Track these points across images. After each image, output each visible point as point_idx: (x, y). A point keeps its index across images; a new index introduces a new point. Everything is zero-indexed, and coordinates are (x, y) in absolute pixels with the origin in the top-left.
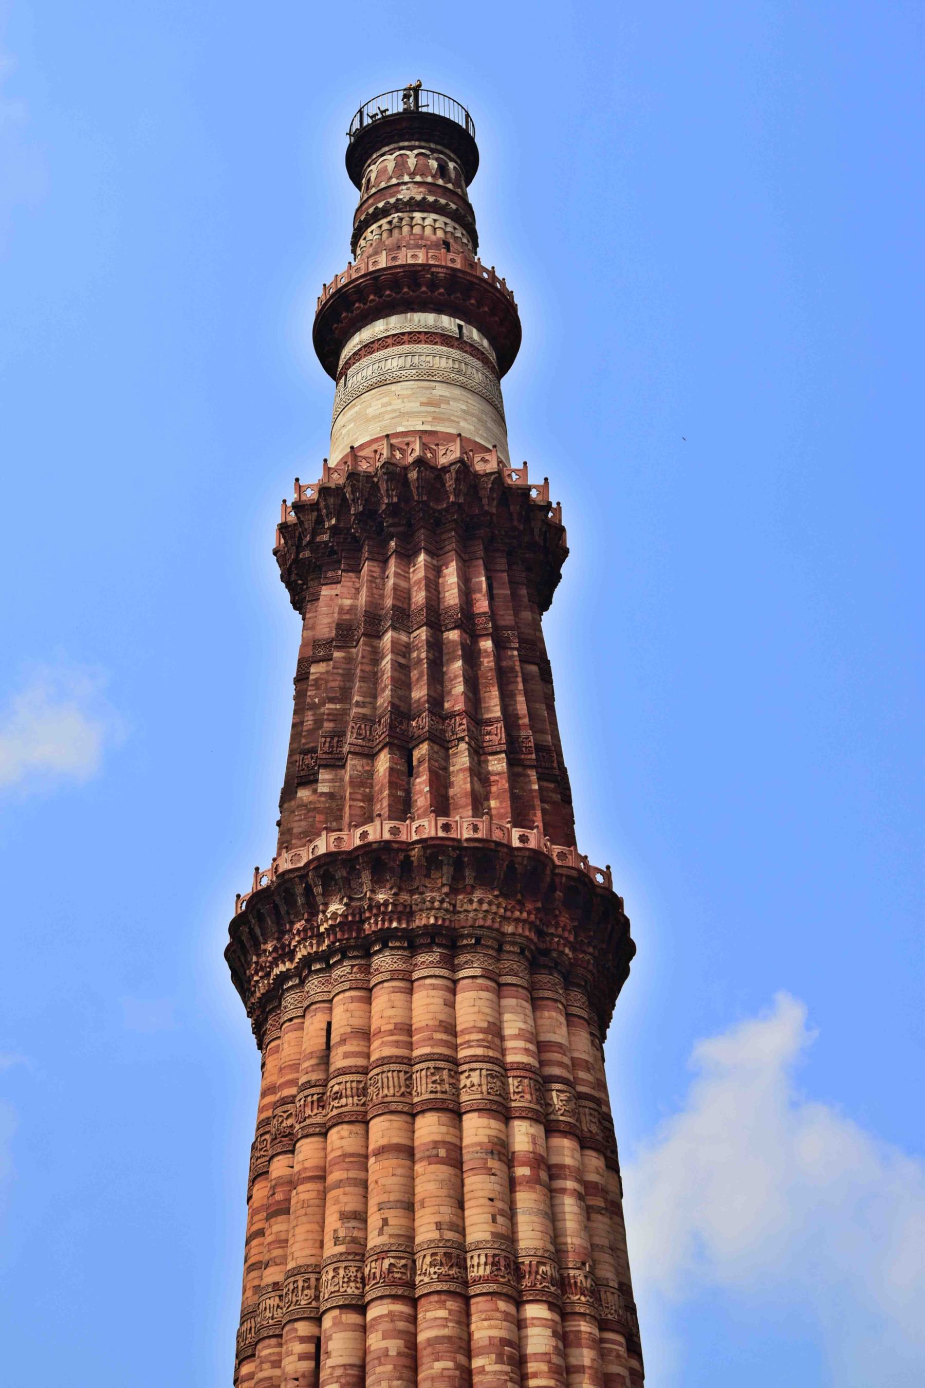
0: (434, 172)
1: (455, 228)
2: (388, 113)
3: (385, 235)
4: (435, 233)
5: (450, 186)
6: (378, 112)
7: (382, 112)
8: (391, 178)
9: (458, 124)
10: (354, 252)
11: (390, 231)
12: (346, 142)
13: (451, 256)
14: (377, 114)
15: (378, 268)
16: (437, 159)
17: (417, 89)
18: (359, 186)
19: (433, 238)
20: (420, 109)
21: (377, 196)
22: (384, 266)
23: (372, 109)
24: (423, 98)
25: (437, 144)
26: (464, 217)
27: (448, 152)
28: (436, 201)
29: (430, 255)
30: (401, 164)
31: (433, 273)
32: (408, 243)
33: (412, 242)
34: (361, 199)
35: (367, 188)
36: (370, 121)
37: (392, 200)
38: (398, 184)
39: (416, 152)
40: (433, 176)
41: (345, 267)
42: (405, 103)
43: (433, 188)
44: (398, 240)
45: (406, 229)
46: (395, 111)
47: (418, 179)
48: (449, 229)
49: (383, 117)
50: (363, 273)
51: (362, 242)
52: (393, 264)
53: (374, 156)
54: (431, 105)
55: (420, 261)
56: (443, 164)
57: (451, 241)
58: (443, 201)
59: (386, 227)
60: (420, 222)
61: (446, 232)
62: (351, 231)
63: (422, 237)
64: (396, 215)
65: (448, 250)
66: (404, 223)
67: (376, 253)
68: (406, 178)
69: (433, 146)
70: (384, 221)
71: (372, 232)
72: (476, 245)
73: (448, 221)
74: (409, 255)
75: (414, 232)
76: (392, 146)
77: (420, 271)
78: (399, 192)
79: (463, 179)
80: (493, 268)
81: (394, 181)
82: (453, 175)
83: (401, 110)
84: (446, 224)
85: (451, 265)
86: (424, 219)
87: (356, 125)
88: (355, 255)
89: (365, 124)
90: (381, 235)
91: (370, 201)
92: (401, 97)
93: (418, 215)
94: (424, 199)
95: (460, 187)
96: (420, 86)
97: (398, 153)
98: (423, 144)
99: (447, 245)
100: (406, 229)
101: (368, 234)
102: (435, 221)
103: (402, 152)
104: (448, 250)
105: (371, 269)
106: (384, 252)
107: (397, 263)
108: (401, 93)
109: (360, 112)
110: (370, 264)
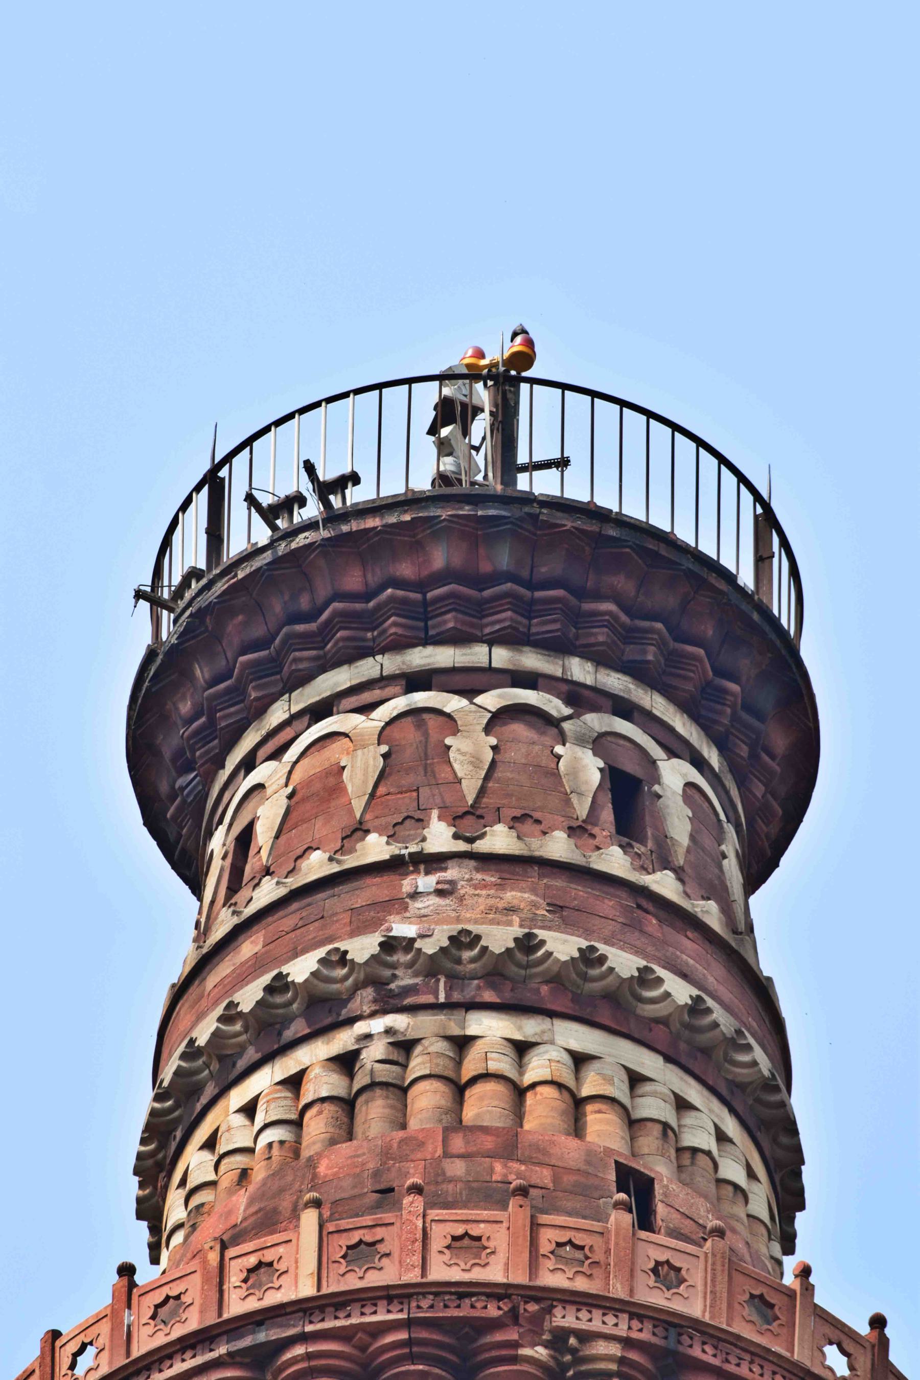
0: (582, 809)
1: (682, 1105)
2: (356, 495)
3: (317, 1126)
4: (577, 1129)
5: (664, 884)
6: (306, 488)
7: (325, 490)
8: (360, 830)
9: (714, 566)
10: (150, 1210)
11: (347, 1105)
12: (133, 635)
13: (655, 1248)
14: (300, 500)
15: (273, 1298)
16: (599, 743)
17: (509, 377)
18: (189, 867)
19: (569, 1150)
20: (522, 482)
21: (286, 921)
22: (307, 1289)
23: (275, 472)
24: (541, 422)
25: (601, 660)
26: (741, 1057)
27: (659, 705)
28: (589, 958)
29: (548, 1238)
30: (412, 758)
31: (558, 1340)
32: (438, 1176)
33: (457, 1168)
34: (202, 930)
35: (235, 881)
36: (262, 534)
37: (363, 948)
38: (395, 866)
39: (492, 700)
40: (577, 831)
41: (101, 1292)
42: (444, 448)
43: (578, 892)
44: (386, 1154)
45: (427, 1100)
46: (393, 487)
47: (499, 839)
48: (651, 1106)
49: (332, 517)
50: (192, 1322)
51: (196, 1162)
52: (352, 1283)
53: (277, 714)
54: (579, 460)
55: (494, 1273)
56: (631, 766)
57: (661, 1170)
58: (624, 962)
59: (323, 1083)
60: (502, 1064)
61: (633, 1124)
62: (140, 1102)
63: (510, 1144)
64: (377, 1025)
65: (645, 1221)
66: (418, 1065)
67: (269, 1220)
68: (439, 837)
69: (580, 670)
70: (313, 1055)
71: (249, 1110)
72: (790, 1197)
73: (649, 1063)
74: (440, 1236)
75: (471, 1112)
76: (368, 668)
77: (494, 1325)
78: (398, 905)
79: (731, 846)
80: (878, 1322)
81: (375, 848)
82: (679, 825)
83: (422, 482)
84: (635, 1079)
85: (657, 1298)
86: (521, 1048)
87: (190, 551)
88: (156, 1229)
89: (236, 545)
90: (297, 1124)
91: (248, 948)
92: (425, 415)
93: (490, 1028)
94: (527, 944)
95: (715, 890)
96: (524, 359)
97: (400, 704)
98: (532, 660)
99: (637, 1188)
100: (427, 1100)
101: (226, 1118)
102: (580, 1060)
103: (421, 698)
104: (645, 1221)
105: (238, 1304)
106: (309, 1219)
107: (374, 1279)
108: (427, 397)
109: (213, 483)
110: (234, 1277)
